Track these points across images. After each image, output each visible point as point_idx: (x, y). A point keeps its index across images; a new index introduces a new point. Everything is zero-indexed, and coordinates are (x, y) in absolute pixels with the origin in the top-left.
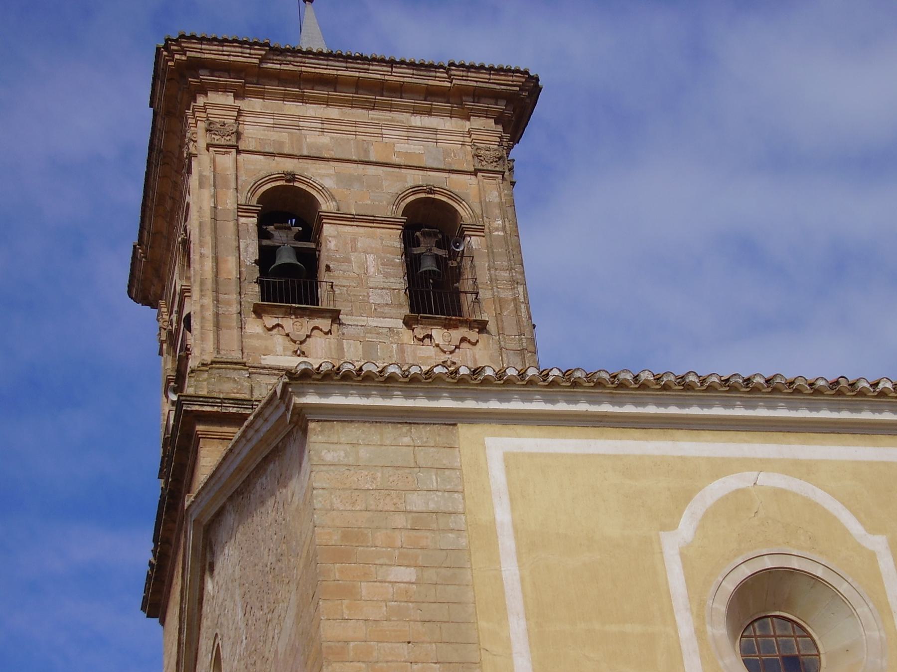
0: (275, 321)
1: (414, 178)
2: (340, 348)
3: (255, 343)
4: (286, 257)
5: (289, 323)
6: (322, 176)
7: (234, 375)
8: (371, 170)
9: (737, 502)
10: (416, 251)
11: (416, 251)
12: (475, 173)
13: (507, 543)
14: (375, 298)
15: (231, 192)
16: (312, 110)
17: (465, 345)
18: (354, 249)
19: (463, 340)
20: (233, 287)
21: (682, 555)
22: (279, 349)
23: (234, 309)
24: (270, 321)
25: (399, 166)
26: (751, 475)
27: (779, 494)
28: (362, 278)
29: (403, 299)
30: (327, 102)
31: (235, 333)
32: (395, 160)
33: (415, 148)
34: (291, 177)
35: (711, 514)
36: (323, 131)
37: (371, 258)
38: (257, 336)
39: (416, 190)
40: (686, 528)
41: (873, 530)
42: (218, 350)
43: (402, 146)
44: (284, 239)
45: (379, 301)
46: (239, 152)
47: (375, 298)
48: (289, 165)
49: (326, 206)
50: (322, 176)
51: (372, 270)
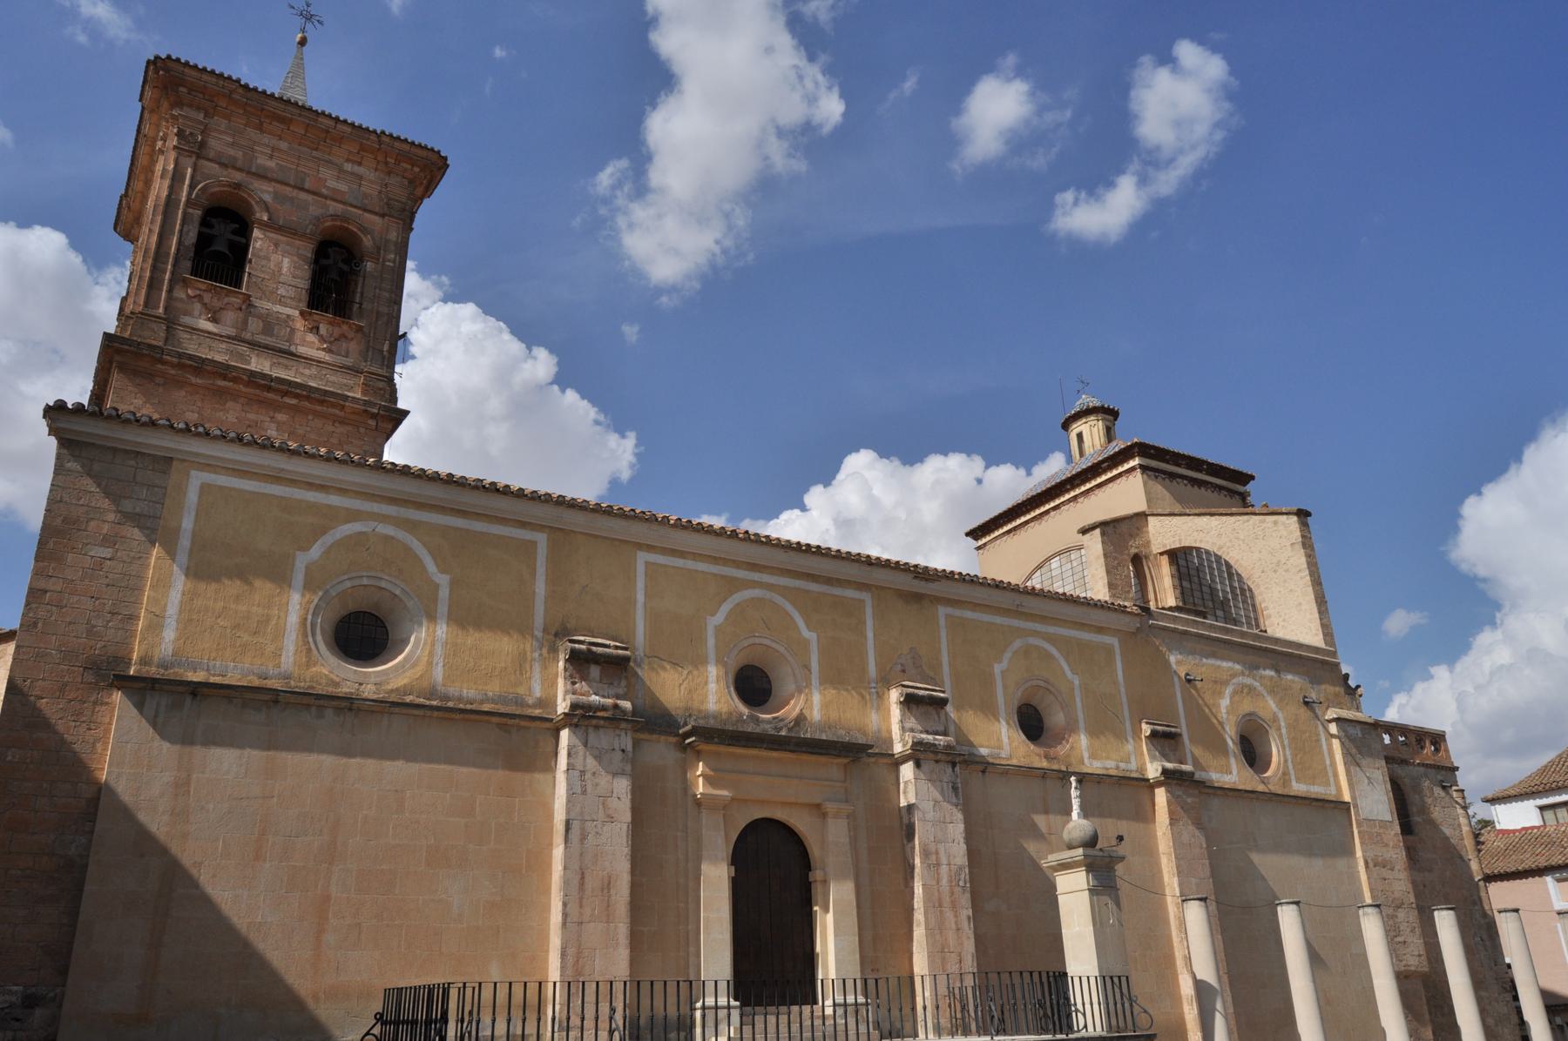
1: (335, 207)
2: (245, 322)
3: (179, 305)
4: (220, 246)
6: (263, 191)
7: (154, 326)
8: (303, 196)
9: (359, 540)
10: (324, 262)
11: (324, 262)
12: (383, 216)
21: (307, 567)
25: (326, 198)
26: (373, 524)
27: (388, 539)
29: (305, 296)
33: (343, 187)
34: (238, 186)
35: (338, 544)
36: (271, 157)
38: (181, 300)
39: (334, 217)
40: (315, 552)
41: (442, 571)
43: (332, 183)
46: (199, 157)
48: (238, 177)
50: (263, 191)
51: (285, 270)
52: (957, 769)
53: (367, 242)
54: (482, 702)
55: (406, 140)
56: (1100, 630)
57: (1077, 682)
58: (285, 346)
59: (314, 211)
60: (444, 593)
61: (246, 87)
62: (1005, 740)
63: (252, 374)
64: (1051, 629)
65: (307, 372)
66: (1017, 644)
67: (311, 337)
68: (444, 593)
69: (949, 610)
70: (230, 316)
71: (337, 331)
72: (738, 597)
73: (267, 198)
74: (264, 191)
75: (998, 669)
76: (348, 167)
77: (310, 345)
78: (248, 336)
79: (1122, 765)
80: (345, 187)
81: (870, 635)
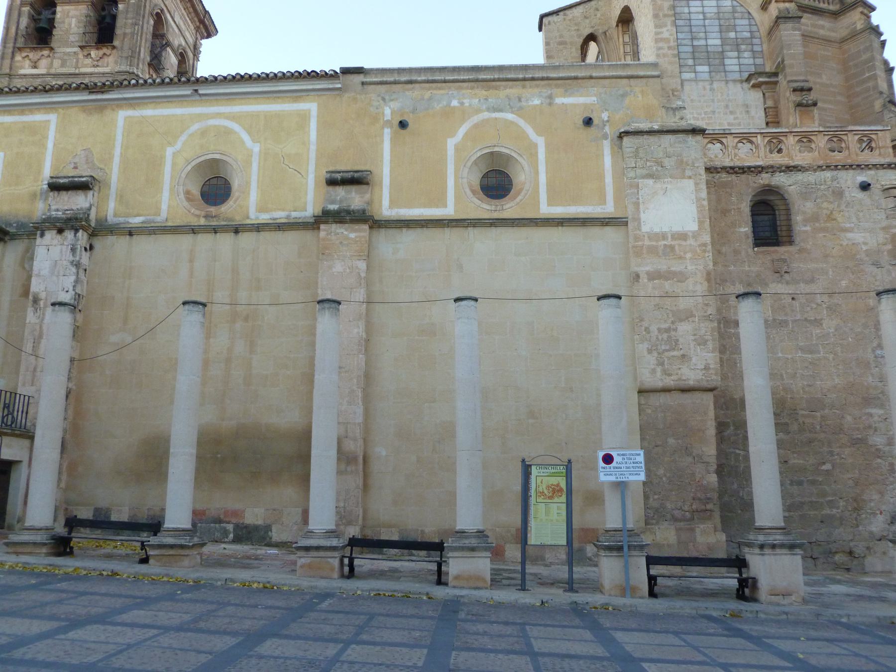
0: (26, 54)
2: (52, 63)
3: (18, 64)
4: (43, 25)
5: (31, 55)
11: (103, 13)
14: (72, 38)
17: (105, 57)
18: (68, 16)
19: (105, 54)
20: (12, 41)
22: (27, 66)
23: (10, 50)
24: (24, 54)
28: (67, 31)
37: (74, 20)
38: (19, 61)
44: (46, 14)
45: (73, 40)
47: (72, 38)
51: (73, 25)
57: (256, 148)
58: (72, 71)
62: (164, 207)
66: (195, 127)
67: (88, 61)
69: (130, 112)
70: (44, 63)
71: (101, 52)
75: (169, 151)
77: (86, 66)
78: (53, 71)
79: (294, 214)
81: (50, 145)
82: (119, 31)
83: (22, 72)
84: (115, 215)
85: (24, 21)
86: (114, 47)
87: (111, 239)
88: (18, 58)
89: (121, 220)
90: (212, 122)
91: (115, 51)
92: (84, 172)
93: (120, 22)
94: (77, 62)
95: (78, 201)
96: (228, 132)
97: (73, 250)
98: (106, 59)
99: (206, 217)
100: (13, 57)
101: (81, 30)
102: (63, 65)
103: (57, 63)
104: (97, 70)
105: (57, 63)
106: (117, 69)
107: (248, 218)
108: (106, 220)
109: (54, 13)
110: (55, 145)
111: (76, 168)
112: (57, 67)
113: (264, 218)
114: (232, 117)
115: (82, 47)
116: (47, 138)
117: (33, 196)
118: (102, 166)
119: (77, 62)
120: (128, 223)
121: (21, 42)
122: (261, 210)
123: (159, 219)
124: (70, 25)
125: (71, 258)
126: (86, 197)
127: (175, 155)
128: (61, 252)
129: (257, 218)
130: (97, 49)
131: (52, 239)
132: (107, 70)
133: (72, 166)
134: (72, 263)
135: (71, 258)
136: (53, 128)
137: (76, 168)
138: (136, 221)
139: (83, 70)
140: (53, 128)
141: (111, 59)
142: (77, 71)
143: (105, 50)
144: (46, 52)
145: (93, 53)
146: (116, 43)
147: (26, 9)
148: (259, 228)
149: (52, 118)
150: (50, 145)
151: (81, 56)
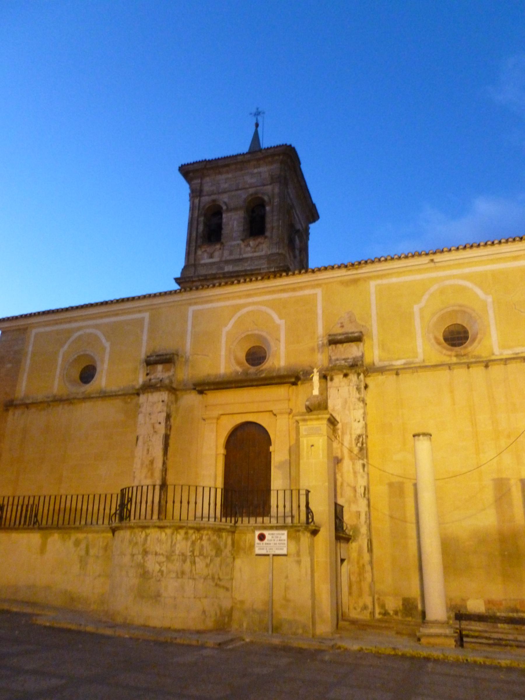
1: (251, 191)
2: (223, 253)
5: (208, 249)
8: (239, 192)
9: (80, 338)
13: (29, 356)
14: (234, 235)
15: (197, 211)
16: (224, 176)
23: (194, 248)
24: (203, 250)
30: (227, 172)
31: (193, 256)
32: (247, 186)
33: (253, 180)
34: (214, 201)
36: (226, 182)
37: (235, 223)
39: (251, 195)
40: (66, 347)
42: (195, 260)
48: (214, 197)
49: (224, 208)
51: (235, 225)
52: (362, 376)
53: (266, 198)
54: (119, 391)
55: (271, 147)
56: (516, 258)
57: (490, 299)
58: (237, 257)
59: (244, 196)
60: (108, 350)
61: (209, 161)
62: (420, 350)
63: (228, 272)
64: (467, 270)
65: (246, 264)
67: (249, 249)
68: (108, 350)
69: (379, 282)
70: (217, 254)
72: (238, 314)
73: (226, 200)
74: (225, 198)
75: (416, 309)
76: (256, 171)
78: (224, 259)
80: (259, 179)
81: (320, 311)
82: (268, 226)
83: (203, 262)
84: (380, 360)
85: (201, 228)
86: (266, 237)
87: (380, 378)
88: (199, 252)
89: (386, 363)
90: (448, 283)
91: (266, 240)
92: (351, 329)
93: (268, 219)
94: (240, 251)
95: (352, 351)
96: (463, 289)
97: (358, 389)
98: (261, 247)
99: (457, 356)
100: (196, 252)
101: (241, 228)
102: (231, 253)
103: (226, 253)
104: (256, 254)
105: (226, 253)
106: (269, 253)
107: (493, 354)
108: (374, 364)
109: (221, 218)
110: (323, 312)
111: (342, 327)
112: (226, 256)
113: (507, 353)
114: (465, 277)
115: (243, 240)
116: (316, 306)
117: (313, 350)
118: (364, 324)
119: (240, 251)
120: (392, 365)
121: (200, 241)
122: (503, 347)
123: (417, 360)
124: (233, 225)
125: (358, 396)
126: (358, 348)
127: (421, 310)
128: (349, 391)
129: (501, 354)
130: (254, 240)
131: (340, 382)
132: (263, 253)
133: (340, 325)
134: (359, 399)
135: (358, 396)
136: (320, 298)
137: (342, 327)
138: (399, 363)
139: (245, 256)
140: (320, 298)
141: (264, 246)
142: (241, 257)
143: (260, 240)
144: (218, 246)
145: (252, 243)
146: (268, 234)
147: (202, 219)
148: (506, 361)
149: (318, 291)
150: (320, 311)
151: (242, 246)
